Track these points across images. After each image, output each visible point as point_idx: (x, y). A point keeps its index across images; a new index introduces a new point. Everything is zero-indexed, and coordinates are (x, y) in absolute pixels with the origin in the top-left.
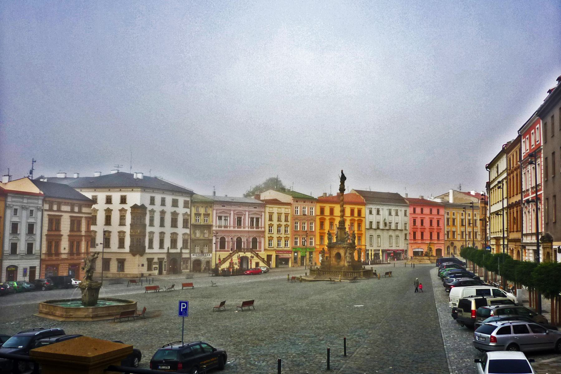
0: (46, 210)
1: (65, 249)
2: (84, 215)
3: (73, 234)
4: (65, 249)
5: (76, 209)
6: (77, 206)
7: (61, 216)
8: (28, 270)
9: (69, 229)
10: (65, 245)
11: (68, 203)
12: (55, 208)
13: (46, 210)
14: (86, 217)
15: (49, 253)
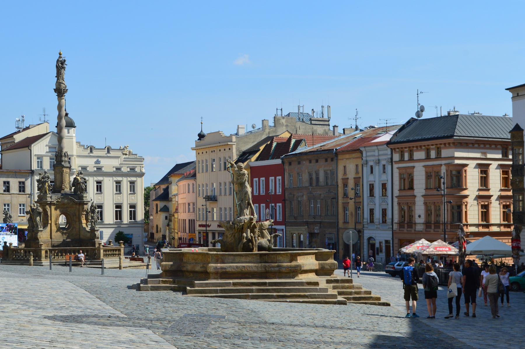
0: (396, 162)
1: (419, 216)
2: (443, 162)
3: (430, 192)
4: (419, 216)
5: (433, 154)
6: (433, 149)
7: (414, 167)
8: (384, 245)
9: (424, 186)
10: (419, 209)
11: (421, 146)
12: (406, 156)
13: (396, 162)
14: (445, 164)
15: (401, 224)
